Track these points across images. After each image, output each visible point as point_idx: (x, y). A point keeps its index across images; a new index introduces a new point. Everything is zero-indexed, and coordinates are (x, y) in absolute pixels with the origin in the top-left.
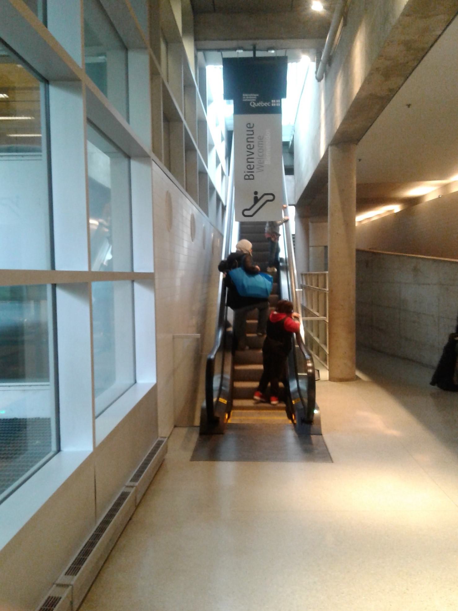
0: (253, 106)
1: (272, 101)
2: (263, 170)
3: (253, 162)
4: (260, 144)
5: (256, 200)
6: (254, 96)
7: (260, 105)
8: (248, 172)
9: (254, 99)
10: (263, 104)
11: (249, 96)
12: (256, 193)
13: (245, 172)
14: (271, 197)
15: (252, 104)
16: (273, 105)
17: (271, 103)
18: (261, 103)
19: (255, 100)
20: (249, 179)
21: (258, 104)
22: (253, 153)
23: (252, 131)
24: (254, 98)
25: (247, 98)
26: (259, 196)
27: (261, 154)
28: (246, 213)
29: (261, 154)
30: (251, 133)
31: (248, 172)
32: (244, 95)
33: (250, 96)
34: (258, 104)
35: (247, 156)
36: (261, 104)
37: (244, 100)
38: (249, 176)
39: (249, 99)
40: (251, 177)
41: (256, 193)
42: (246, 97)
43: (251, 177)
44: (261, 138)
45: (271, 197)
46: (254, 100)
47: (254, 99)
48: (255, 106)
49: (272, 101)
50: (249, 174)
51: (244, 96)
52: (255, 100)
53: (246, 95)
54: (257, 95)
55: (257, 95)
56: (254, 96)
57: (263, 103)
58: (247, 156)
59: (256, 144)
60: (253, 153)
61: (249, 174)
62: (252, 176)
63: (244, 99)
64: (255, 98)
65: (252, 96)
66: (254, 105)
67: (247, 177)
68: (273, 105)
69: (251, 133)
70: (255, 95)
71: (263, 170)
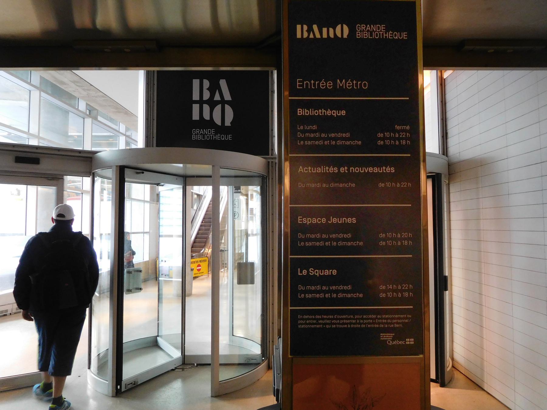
0: (390, 344)
1: (407, 340)
6: (390, 335)
9: (390, 338)
11: (385, 336)
15: (389, 342)
16: (407, 343)
17: (406, 341)
18: (397, 341)
21: (395, 343)
25: (384, 336)
32: (381, 334)
33: (387, 335)
34: (395, 343)
37: (381, 339)
42: (383, 336)
46: (390, 339)
47: (390, 338)
48: (391, 344)
49: (407, 340)
51: (382, 336)
53: (383, 334)
54: (394, 334)
55: (394, 334)
56: (390, 335)
64: (392, 337)
65: (388, 335)
68: (407, 343)
70: (391, 334)
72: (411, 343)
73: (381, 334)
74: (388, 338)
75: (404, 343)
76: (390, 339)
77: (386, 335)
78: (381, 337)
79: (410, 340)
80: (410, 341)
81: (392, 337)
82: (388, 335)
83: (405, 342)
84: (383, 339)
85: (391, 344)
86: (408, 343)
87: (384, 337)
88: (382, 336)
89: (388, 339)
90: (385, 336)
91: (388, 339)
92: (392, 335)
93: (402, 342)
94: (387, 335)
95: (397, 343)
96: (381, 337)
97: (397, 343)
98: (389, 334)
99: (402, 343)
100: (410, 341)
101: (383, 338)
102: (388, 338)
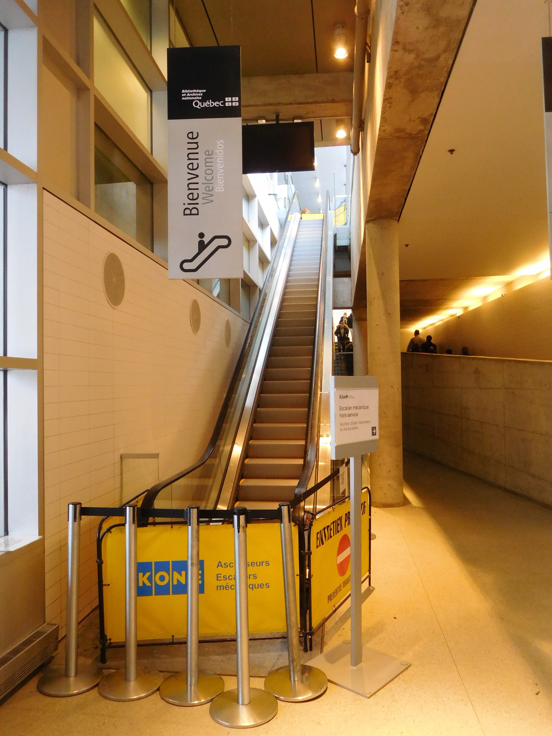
0: (198, 107)
1: (227, 99)
2: (212, 201)
3: (198, 189)
4: (207, 162)
5: (202, 246)
7: (207, 105)
8: (189, 204)
9: (198, 96)
10: (212, 104)
11: (190, 93)
12: (201, 235)
13: (184, 204)
14: (225, 242)
15: (196, 104)
16: (227, 104)
17: (225, 102)
18: (209, 102)
19: (200, 98)
20: (191, 214)
21: (205, 104)
22: (197, 176)
23: (196, 143)
24: (199, 95)
25: (188, 95)
26: (206, 240)
27: (209, 177)
28: (186, 266)
29: (209, 177)
30: (195, 146)
31: (189, 204)
32: (183, 91)
33: (192, 93)
34: (205, 104)
35: (188, 179)
36: (209, 104)
37: (183, 99)
38: (191, 211)
39: (191, 96)
40: (194, 211)
41: (201, 235)
42: (187, 93)
43: (194, 211)
44: (209, 154)
45: (225, 242)
46: (198, 98)
47: (198, 96)
48: (200, 106)
49: (227, 99)
50: (191, 207)
51: (184, 93)
52: (200, 98)
53: (187, 91)
54: (205, 91)
55: (205, 91)
57: (213, 103)
58: (188, 179)
59: (201, 162)
60: (197, 176)
61: (191, 207)
62: (196, 210)
63: (184, 97)
64: (202, 94)
65: (195, 93)
66: (200, 105)
67: (188, 212)
68: (227, 104)
69: (195, 146)
70: (200, 91)
71: (212, 201)
72: (230, 98)
73: (183, 91)
74: (194, 97)
75: (222, 104)
76: (198, 98)
77: (191, 91)
78: (183, 95)
79: (232, 99)
80: (232, 102)
81: (202, 94)
82: (195, 93)
83: (224, 103)
84: (187, 98)
85: (200, 106)
86: (229, 104)
87: (188, 96)
88: (184, 93)
89: (195, 98)
90: (190, 93)
91: (195, 98)
92: (201, 93)
93: (218, 103)
94: (192, 93)
95: (209, 105)
96: (183, 95)
97: (209, 105)
98: (198, 91)
99: (219, 105)
100: (232, 102)
101: (186, 97)
102: (194, 97)
